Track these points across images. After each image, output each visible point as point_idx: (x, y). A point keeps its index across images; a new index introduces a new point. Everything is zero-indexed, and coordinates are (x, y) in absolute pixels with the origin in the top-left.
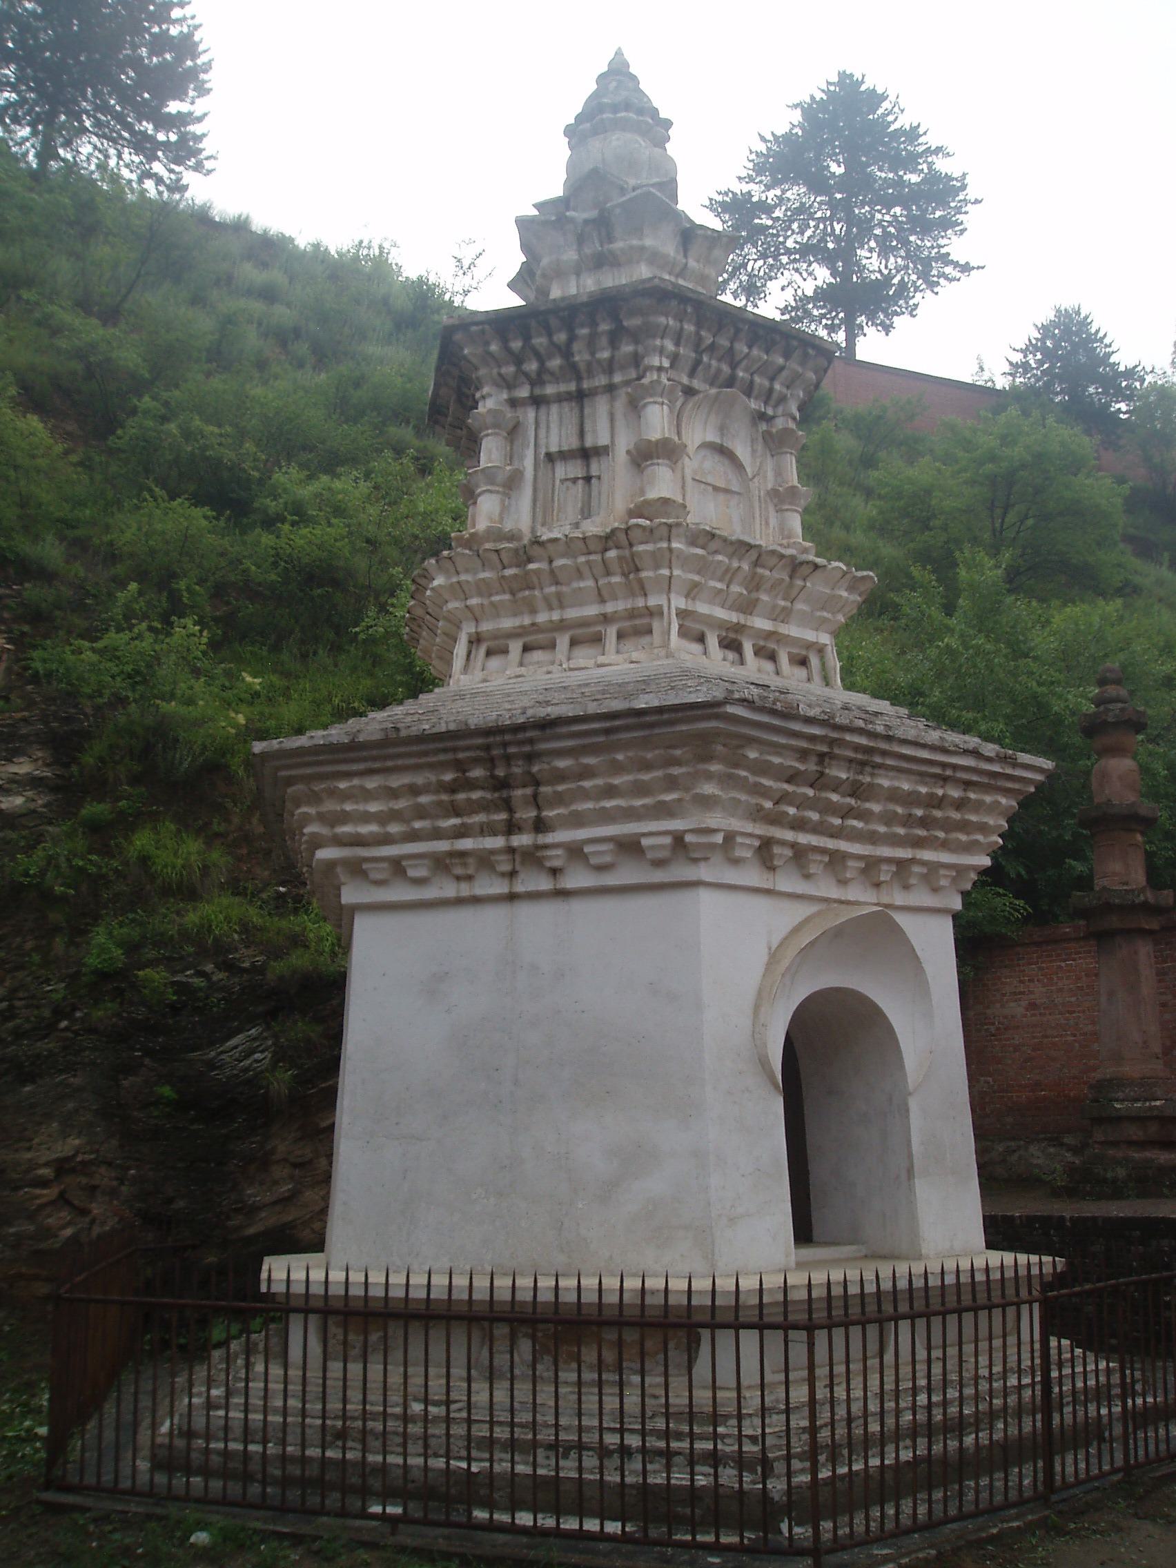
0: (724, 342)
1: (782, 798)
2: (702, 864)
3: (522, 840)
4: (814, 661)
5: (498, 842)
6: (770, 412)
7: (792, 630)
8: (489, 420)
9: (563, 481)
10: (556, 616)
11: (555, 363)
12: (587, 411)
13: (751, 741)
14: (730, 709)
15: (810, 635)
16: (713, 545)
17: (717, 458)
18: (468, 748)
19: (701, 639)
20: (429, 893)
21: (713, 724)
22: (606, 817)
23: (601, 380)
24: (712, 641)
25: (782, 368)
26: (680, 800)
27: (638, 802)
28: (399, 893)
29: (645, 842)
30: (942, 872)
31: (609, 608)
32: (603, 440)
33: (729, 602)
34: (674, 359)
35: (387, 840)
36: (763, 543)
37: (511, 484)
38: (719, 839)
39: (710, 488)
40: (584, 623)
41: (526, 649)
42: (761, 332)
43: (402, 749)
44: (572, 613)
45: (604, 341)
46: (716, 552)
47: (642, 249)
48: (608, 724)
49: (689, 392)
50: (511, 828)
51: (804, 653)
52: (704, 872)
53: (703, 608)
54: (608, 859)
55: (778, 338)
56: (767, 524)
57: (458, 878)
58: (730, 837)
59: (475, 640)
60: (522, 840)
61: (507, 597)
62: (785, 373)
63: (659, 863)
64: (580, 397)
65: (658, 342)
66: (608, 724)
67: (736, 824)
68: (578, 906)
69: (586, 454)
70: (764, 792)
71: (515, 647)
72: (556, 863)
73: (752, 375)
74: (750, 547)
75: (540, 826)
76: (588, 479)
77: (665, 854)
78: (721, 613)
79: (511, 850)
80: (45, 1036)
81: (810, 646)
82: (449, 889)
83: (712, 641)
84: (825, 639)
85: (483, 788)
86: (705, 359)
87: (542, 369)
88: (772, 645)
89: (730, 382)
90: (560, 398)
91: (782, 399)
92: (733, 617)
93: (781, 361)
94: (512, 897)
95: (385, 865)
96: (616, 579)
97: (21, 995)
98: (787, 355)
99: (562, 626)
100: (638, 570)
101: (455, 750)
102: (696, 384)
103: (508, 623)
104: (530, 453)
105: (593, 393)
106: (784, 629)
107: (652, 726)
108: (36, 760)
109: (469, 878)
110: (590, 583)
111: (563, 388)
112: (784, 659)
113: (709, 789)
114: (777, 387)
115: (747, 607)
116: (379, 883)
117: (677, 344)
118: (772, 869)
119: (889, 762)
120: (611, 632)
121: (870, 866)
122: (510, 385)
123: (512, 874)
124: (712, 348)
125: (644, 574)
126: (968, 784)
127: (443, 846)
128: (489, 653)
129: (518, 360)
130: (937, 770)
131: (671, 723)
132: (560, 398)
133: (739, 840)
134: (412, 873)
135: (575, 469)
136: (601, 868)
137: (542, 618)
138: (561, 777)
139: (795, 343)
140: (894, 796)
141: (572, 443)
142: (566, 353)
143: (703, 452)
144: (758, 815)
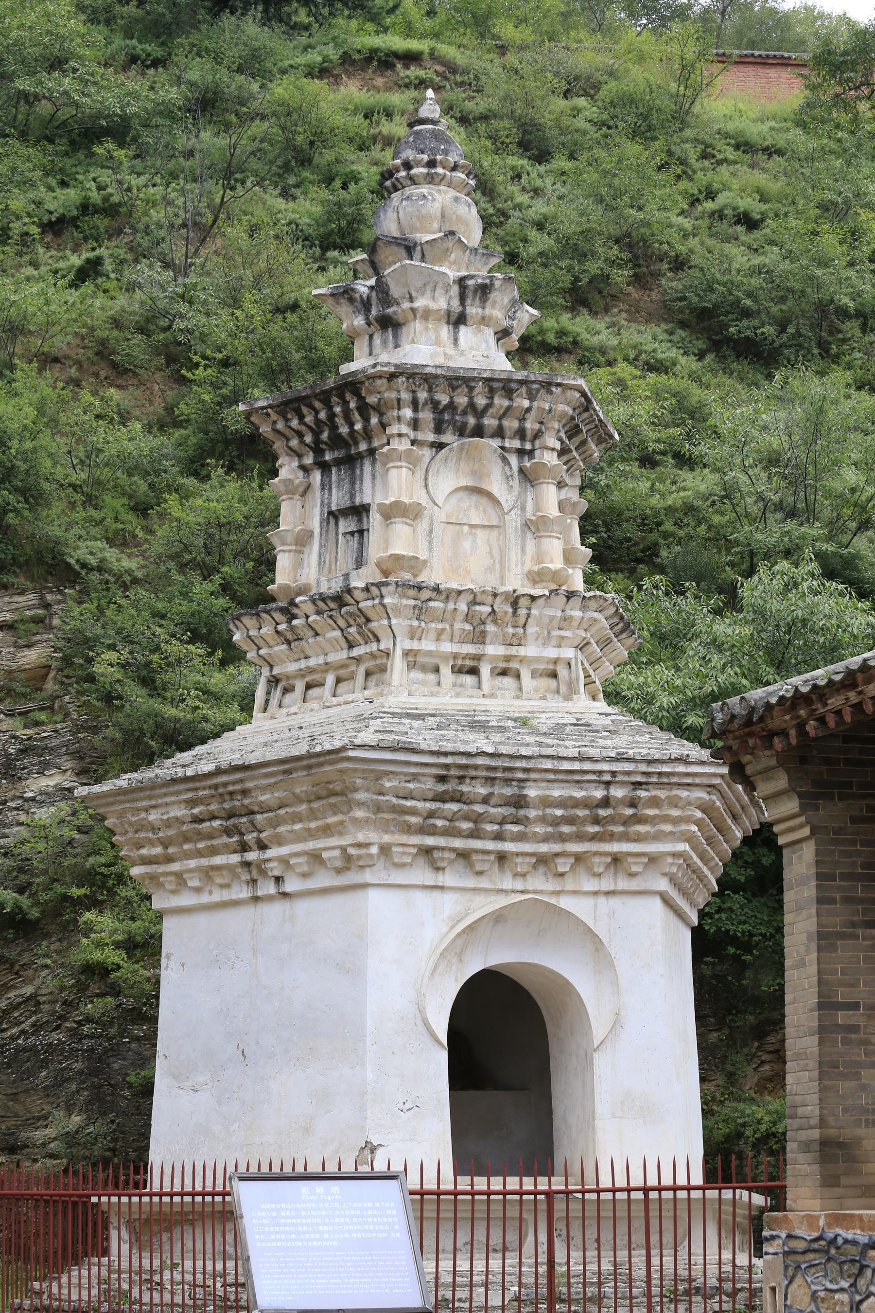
0: (462, 400)
1: (431, 815)
2: (368, 870)
3: (251, 856)
4: (562, 672)
5: (235, 858)
6: (528, 446)
7: (530, 650)
8: (282, 488)
9: (345, 534)
10: (321, 660)
11: (325, 436)
12: (358, 471)
13: (387, 773)
14: (351, 753)
15: (551, 652)
16: (425, 594)
17: (474, 497)
18: (204, 788)
19: (437, 670)
20: (205, 899)
21: (345, 765)
22: (299, 838)
23: (363, 447)
24: (446, 670)
25: (528, 410)
26: (341, 823)
27: (313, 825)
28: (186, 900)
29: (325, 855)
30: (630, 860)
31: (355, 652)
32: (367, 500)
33: (456, 639)
34: (415, 424)
35: (169, 860)
36: (471, 586)
37: (303, 540)
38: (374, 850)
39: (466, 528)
40: (343, 666)
41: (309, 687)
42: (495, 385)
43: (164, 790)
44: (332, 658)
45: (357, 416)
46: (430, 599)
47: (413, 310)
48: (286, 767)
49: (440, 446)
50: (244, 848)
51: (551, 667)
52: (368, 876)
53: (427, 645)
54: (305, 868)
55: (514, 385)
56: (523, 551)
57: (222, 886)
58: (385, 850)
59: (274, 681)
60: (251, 856)
61: (284, 647)
62: (533, 412)
63: (339, 871)
64: (351, 462)
65: (395, 413)
66: (286, 767)
67: (387, 838)
68: (302, 906)
69: (359, 511)
70: (413, 812)
71: (300, 686)
72: (277, 873)
73: (500, 419)
74: (460, 592)
75: (262, 846)
76: (361, 532)
77: (339, 864)
78: (447, 647)
79: (247, 864)
80: (58, 1027)
81: (556, 662)
82: (217, 896)
83: (446, 670)
84: (569, 653)
85: (221, 818)
86: (446, 417)
87: (317, 441)
88: (514, 665)
89: (479, 432)
90: (338, 462)
91: (537, 435)
92: (469, 649)
93: (526, 403)
94: (256, 899)
95: (172, 878)
96: (353, 630)
97: (43, 992)
98: (532, 397)
99: (327, 667)
100: (368, 620)
101: (197, 789)
102: (444, 439)
103: (292, 667)
104: (317, 511)
105: (360, 456)
106: (522, 651)
107: (309, 767)
108: (65, 771)
109: (227, 886)
110: (337, 633)
111: (336, 454)
112: (525, 675)
113: (360, 813)
114: (528, 425)
115: (480, 638)
116: (174, 892)
117: (416, 409)
118: (438, 869)
119: (533, 776)
120: (330, 679)
121: (543, 860)
122: (300, 456)
123: (254, 881)
124: (451, 406)
125: (373, 625)
126: (637, 785)
127: (205, 862)
128: (286, 690)
129: (300, 435)
130: (593, 777)
131: (321, 765)
132: (338, 462)
133: (395, 849)
134: (190, 884)
135: (346, 525)
136: (305, 875)
137: (312, 662)
138: (265, 809)
139: (535, 386)
140: (546, 802)
141: (346, 503)
142: (334, 427)
143: (462, 494)
144: (408, 829)
